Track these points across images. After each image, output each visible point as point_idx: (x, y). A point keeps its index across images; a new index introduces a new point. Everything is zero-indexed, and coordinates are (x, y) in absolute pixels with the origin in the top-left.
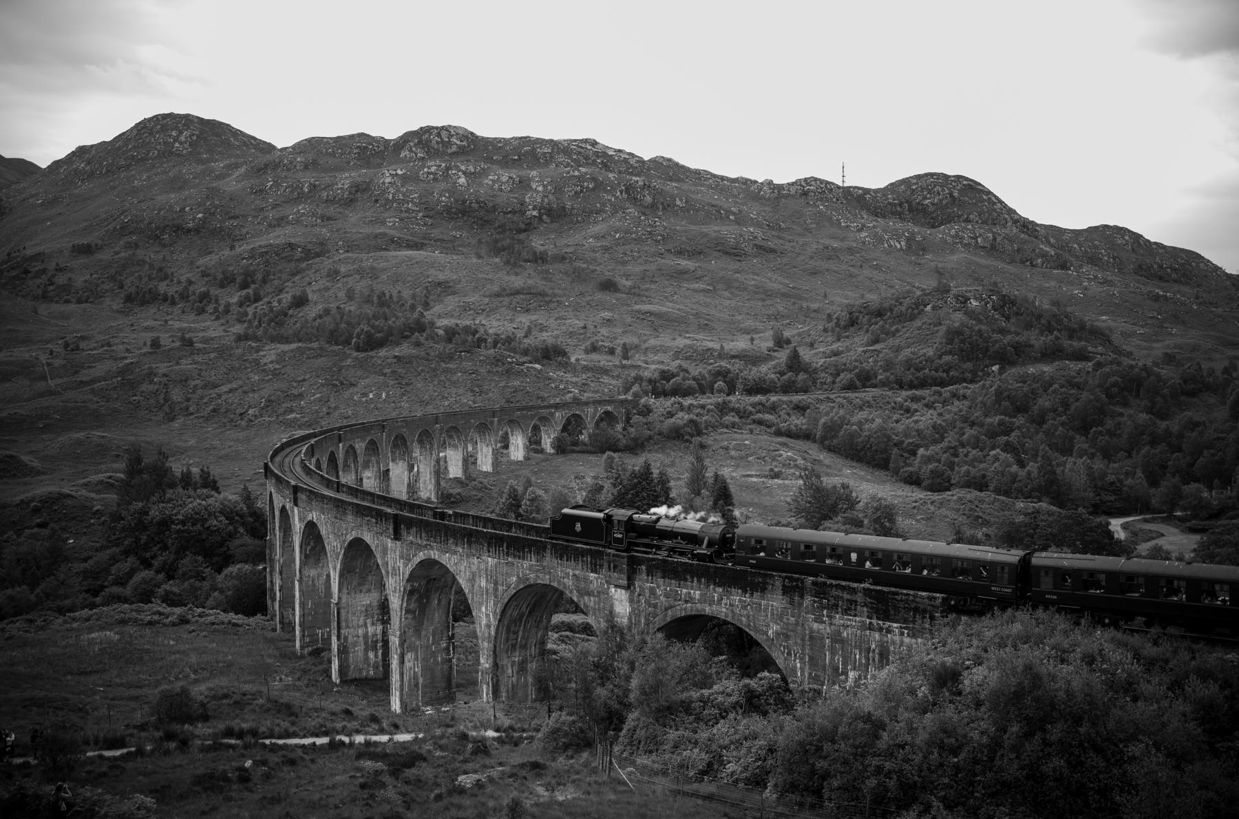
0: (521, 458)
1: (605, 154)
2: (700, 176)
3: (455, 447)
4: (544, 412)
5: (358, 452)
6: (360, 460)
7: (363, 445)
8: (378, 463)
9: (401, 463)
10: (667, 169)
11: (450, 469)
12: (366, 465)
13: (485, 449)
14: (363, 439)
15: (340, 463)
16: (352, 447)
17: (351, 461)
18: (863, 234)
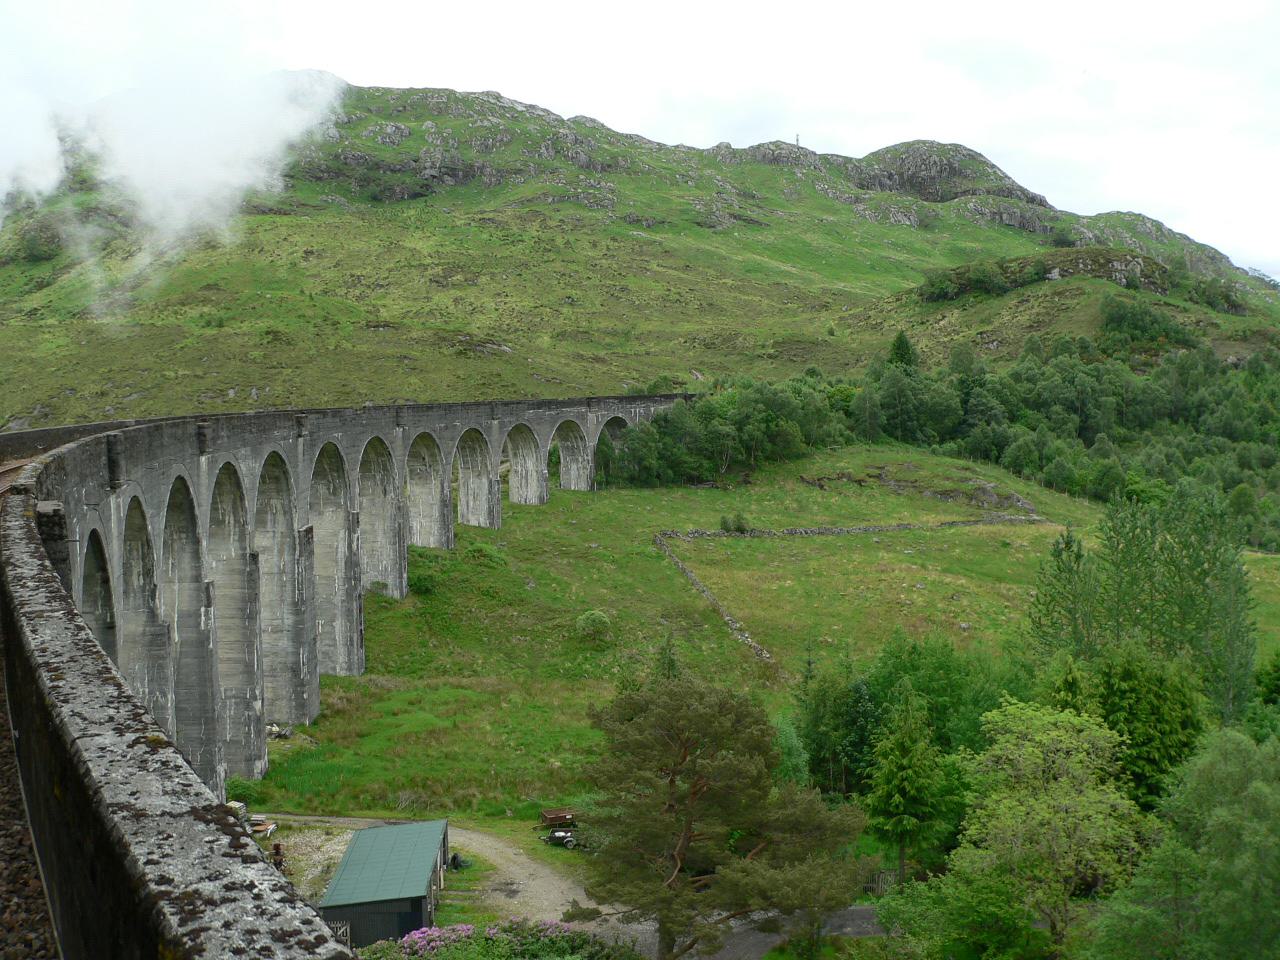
0: (534, 500)
1: (512, 109)
2: (632, 141)
3: (423, 477)
4: (570, 413)
5: (246, 483)
6: (251, 503)
7: (258, 467)
8: (288, 512)
9: (329, 512)
10: (587, 130)
11: (415, 525)
12: (261, 522)
13: (473, 483)
14: (256, 453)
15: (203, 512)
16: (229, 472)
17: (227, 506)
18: (861, 207)
